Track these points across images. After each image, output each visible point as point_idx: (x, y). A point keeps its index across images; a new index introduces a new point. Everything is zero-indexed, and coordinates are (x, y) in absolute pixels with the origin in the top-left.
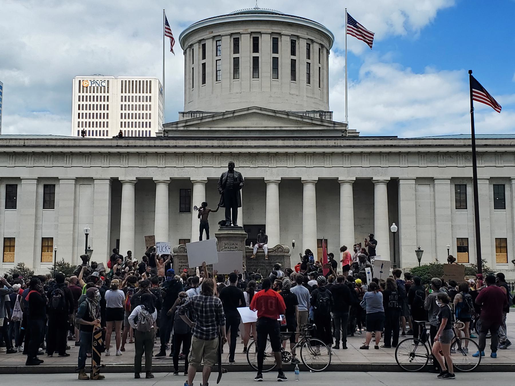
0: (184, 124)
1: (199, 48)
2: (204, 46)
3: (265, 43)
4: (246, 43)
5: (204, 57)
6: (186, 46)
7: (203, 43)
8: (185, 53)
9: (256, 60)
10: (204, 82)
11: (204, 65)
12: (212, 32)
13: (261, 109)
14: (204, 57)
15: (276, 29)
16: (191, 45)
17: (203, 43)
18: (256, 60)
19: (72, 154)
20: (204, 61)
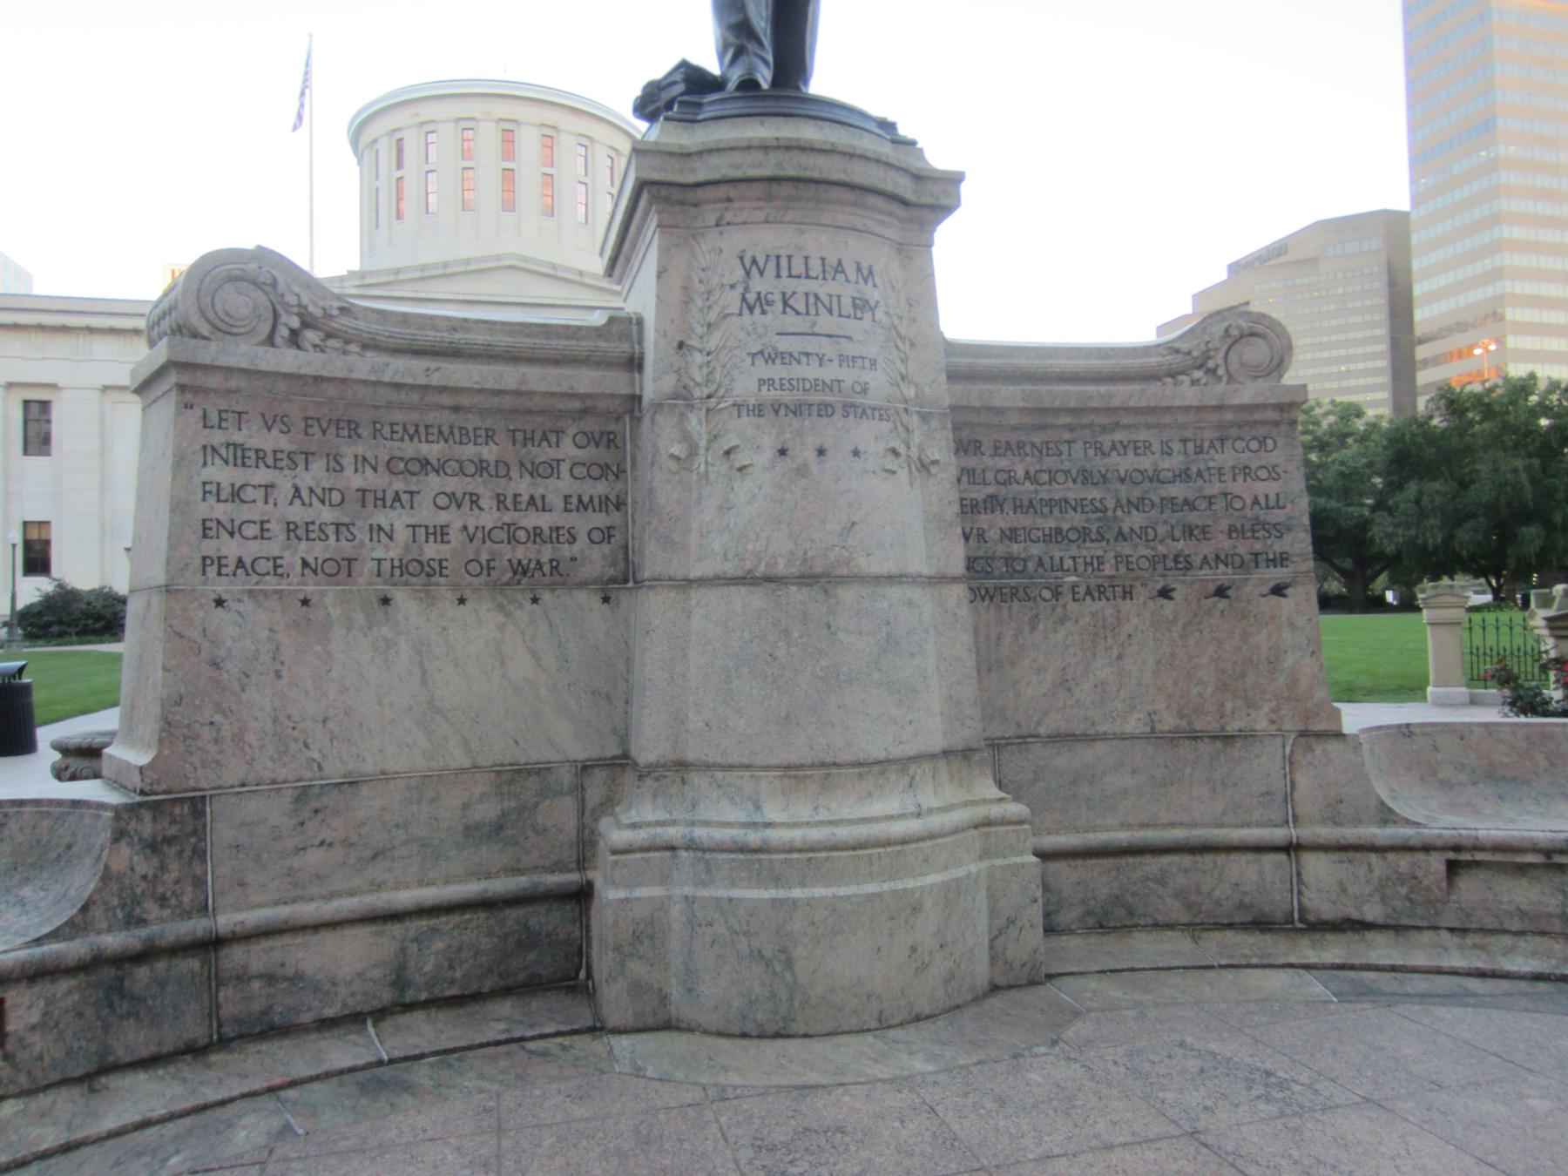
0: (357, 283)
1: (390, 146)
2: (400, 140)
3: (529, 141)
4: (488, 140)
5: (400, 165)
6: (361, 146)
7: (398, 136)
8: (360, 162)
9: (508, 176)
10: (399, 216)
11: (400, 179)
12: (417, 115)
13: (525, 259)
14: (400, 165)
15: (551, 116)
16: (374, 141)
17: (398, 136)
18: (508, 176)
19: (90, 330)
20: (398, 174)
